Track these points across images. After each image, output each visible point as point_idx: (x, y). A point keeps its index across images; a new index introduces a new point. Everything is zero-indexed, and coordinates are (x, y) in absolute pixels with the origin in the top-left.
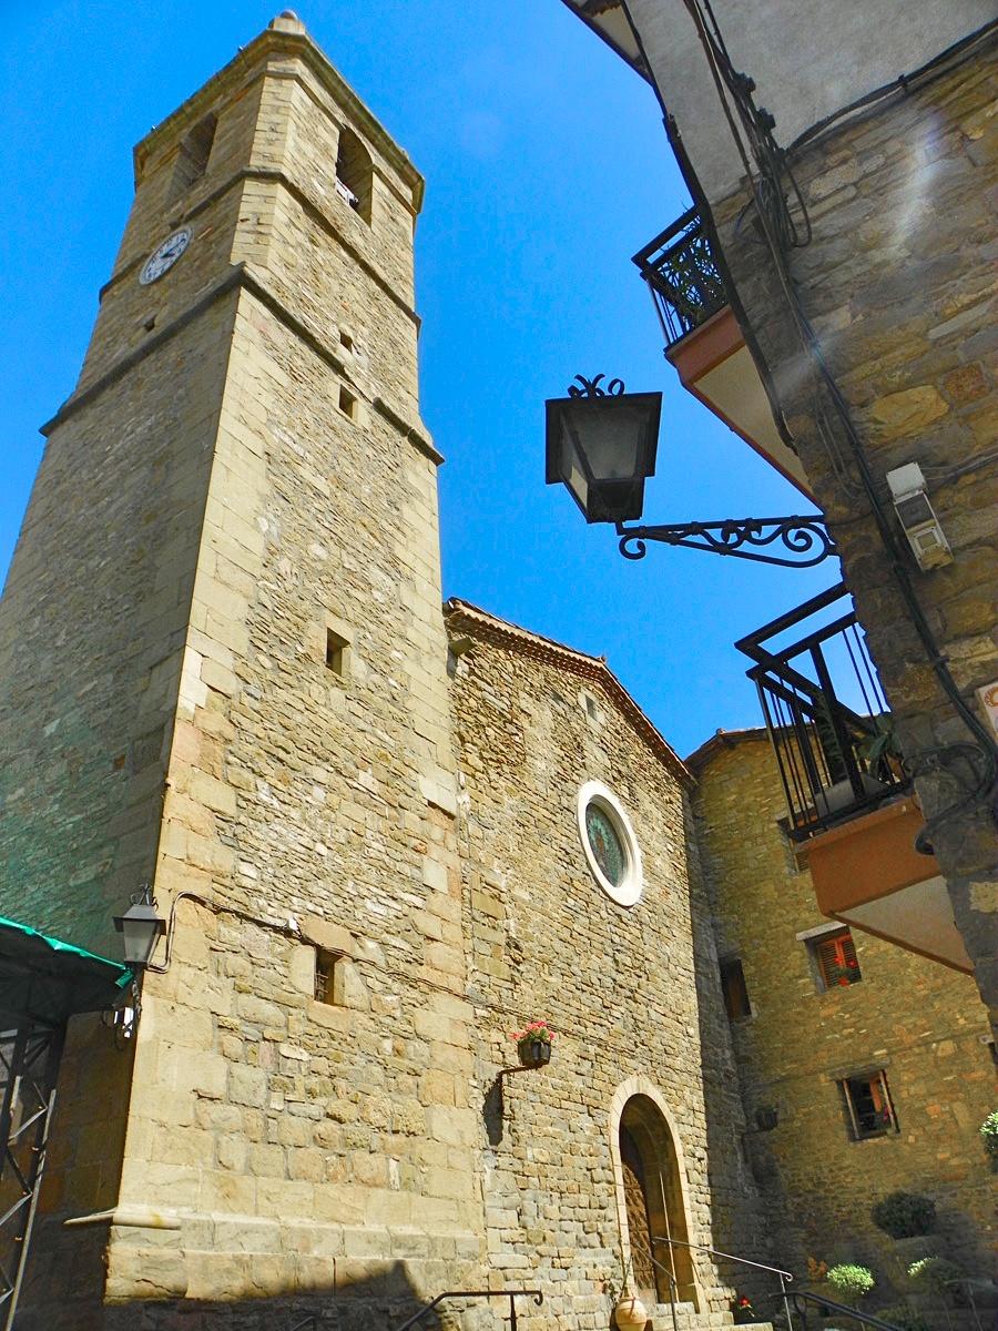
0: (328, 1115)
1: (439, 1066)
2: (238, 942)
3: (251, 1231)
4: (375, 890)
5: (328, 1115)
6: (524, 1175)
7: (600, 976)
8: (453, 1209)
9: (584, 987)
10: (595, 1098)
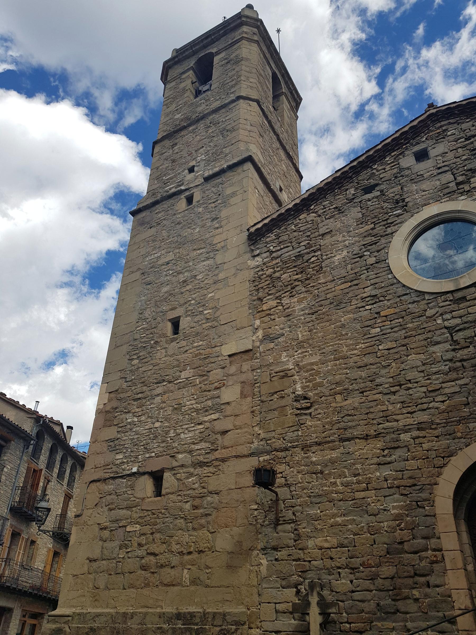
0: (148, 554)
1: (225, 505)
2: (112, 489)
3: (100, 615)
4: (186, 426)
5: (148, 554)
6: (305, 561)
7: (423, 368)
8: (230, 593)
9: (393, 389)
10: (410, 478)
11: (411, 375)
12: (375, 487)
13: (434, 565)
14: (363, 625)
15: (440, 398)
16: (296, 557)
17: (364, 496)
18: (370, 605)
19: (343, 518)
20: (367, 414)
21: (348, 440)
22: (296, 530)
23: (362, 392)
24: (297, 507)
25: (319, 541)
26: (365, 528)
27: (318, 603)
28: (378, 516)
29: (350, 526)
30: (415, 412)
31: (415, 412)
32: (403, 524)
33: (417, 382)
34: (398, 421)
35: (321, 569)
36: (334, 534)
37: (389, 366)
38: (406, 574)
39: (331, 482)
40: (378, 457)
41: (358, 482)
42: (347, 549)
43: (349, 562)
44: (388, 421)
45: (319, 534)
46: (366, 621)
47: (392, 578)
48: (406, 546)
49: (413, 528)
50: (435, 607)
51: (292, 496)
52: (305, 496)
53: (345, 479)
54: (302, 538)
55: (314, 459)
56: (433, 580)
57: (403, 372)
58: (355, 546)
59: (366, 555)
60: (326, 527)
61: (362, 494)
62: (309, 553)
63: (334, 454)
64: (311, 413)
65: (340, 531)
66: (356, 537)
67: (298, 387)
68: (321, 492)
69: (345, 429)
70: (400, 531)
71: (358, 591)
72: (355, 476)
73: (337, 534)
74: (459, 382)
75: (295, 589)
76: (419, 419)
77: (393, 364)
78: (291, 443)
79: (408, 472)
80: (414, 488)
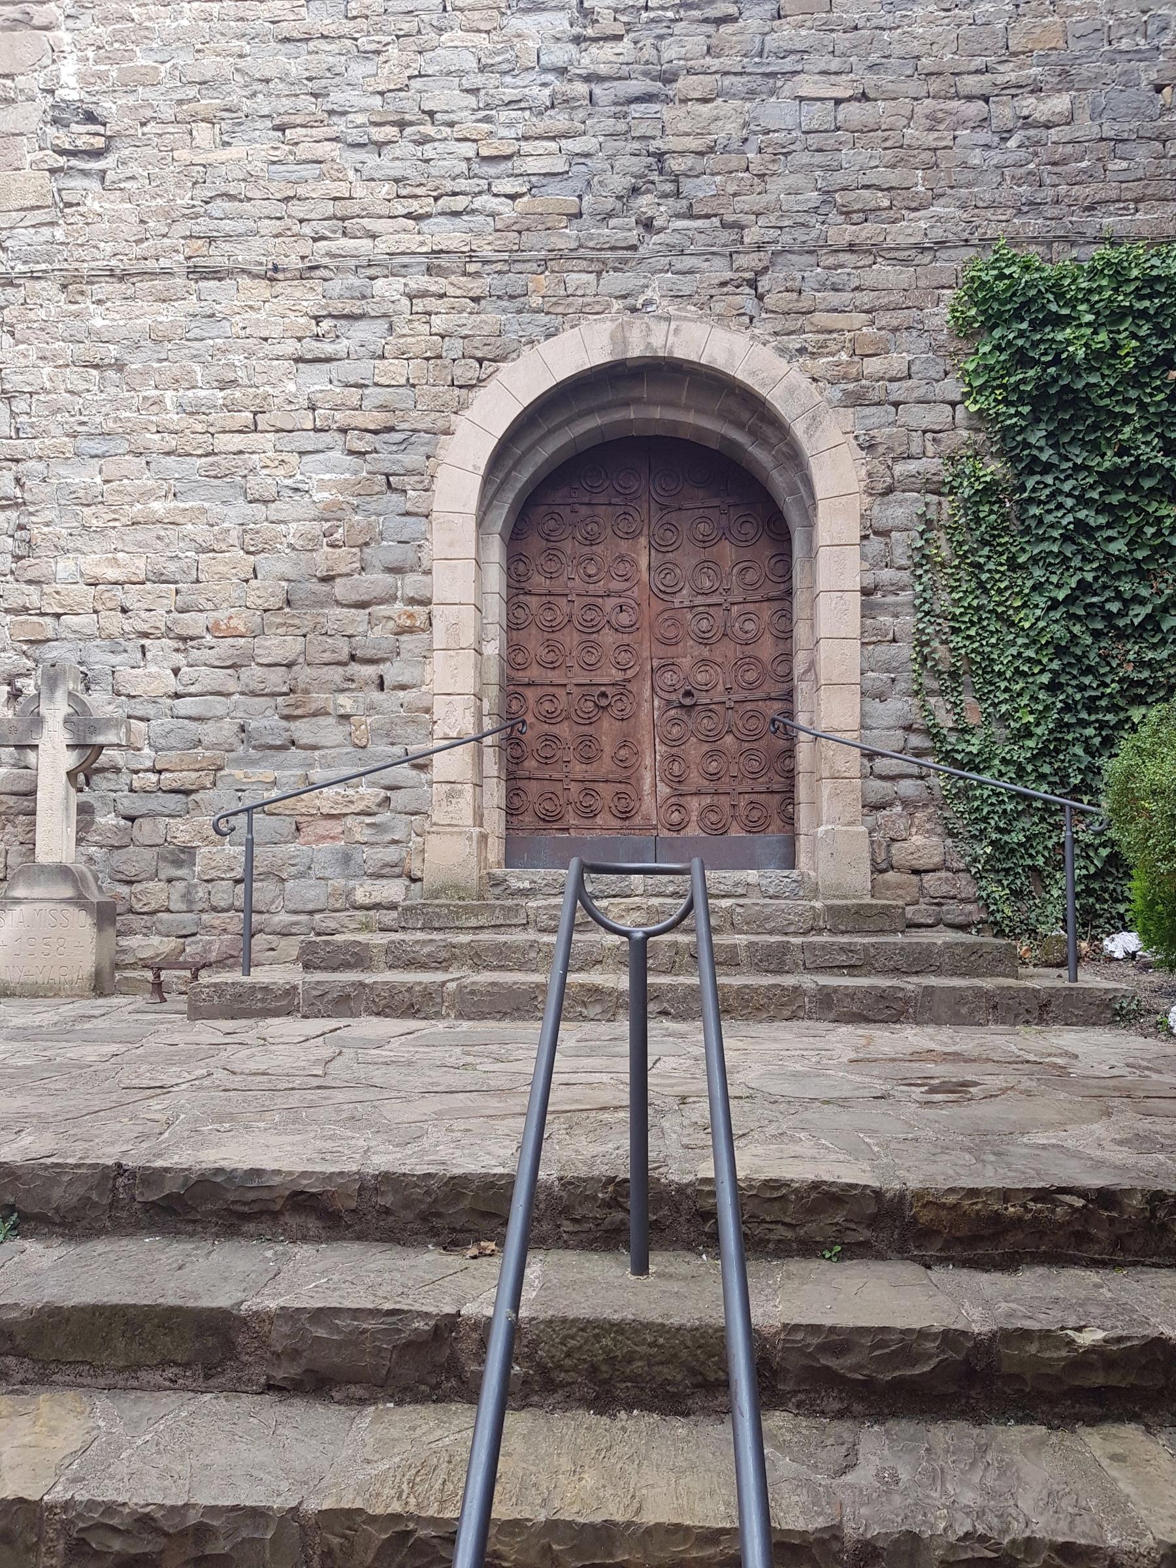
7: (478, 80)
9: (379, 134)
10: (383, 408)
11: (444, 97)
12: (279, 425)
13: (403, 638)
14: (194, 775)
15: (508, 186)
16: (15, 602)
17: (241, 448)
18: (221, 729)
19: (172, 504)
20: (287, 199)
21: (215, 274)
22: (21, 527)
23: (281, 128)
24: (30, 464)
25: (94, 564)
26: (234, 533)
27: (67, 721)
28: (272, 506)
29: (190, 526)
30: (429, 216)
31: (429, 216)
32: (341, 530)
33: (451, 124)
34: (374, 237)
35: (91, 638)
36: (139, 544)
37: (378, 53)
38: (327, 657)
39: (145, 398)
40: (299, 339)
41: (230, 407)
42: (173, 586)
43: (175, 622)
44: (344, 234)
45: (94, 543)
46: (204, 765)
47: (289, 666)
48: (340, 589)
49: (367, 544)
50: (388, 735)
51: (18, 430)
52: (58, 431)
53: (190, 393)
54: (38, 552)
55: (98, 322)
56: (392, 672)
57: (416, 84)
58: (198, 581)
59: (225, 605)
60: (116, 524)
61: (237, 442)
62: (57, 593)
63: (167, 316)
64: (104, 172)
65: (159, 538)
66: (203, 556)
67: (68, 70)
68: (111, 425)
69: (211, 240)
70: (330, 549)
71: (191, 695)
72: (225, 385)
73: (147, 546)
74: (569, 145)
75: (8, 688)
76: (436, 239)
77: (393, 51)
78: (25, 262)
79: (378, 389)
80: (386, 437)
